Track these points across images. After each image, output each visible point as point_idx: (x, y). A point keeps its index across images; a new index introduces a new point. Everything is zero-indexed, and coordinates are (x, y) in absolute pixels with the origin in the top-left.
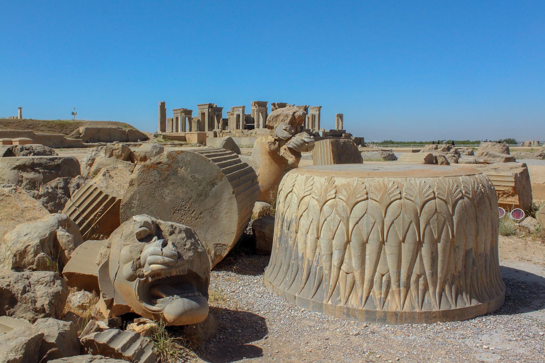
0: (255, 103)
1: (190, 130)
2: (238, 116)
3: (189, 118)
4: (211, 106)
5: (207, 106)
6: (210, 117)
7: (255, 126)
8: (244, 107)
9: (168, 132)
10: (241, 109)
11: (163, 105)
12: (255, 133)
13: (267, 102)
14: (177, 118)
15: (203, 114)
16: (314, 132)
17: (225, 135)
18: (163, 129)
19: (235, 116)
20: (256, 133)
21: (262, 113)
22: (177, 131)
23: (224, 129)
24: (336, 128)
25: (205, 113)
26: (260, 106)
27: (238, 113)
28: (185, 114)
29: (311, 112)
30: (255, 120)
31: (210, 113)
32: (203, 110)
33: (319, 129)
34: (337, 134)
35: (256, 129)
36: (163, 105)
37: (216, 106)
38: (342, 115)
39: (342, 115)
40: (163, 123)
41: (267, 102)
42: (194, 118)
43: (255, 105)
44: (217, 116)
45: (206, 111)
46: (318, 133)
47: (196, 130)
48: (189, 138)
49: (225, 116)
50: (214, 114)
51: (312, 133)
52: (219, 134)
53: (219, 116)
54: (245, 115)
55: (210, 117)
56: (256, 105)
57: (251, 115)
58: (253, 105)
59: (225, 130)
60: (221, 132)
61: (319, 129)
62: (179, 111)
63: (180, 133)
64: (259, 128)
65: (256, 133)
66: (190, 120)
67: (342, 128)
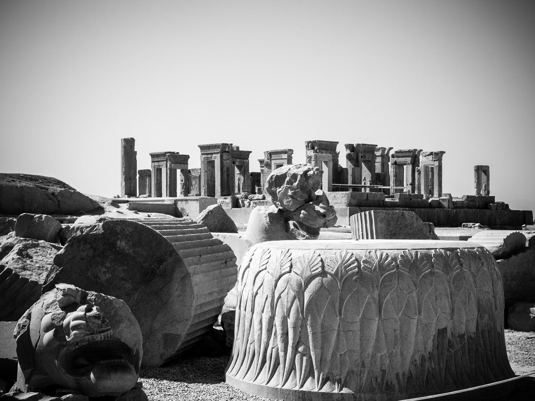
3: (182, 171)
5: (219, 150)
6: (225, 169)
9: (142, 199)
14: (159, 171)
15: (210, 164)
16: (430, 201)
17: (254, 203)
21: (326, 163)
22: (159, 194)
23: (254, 192)
24: (473, 192)
26: (323, 149)
31: (225, 162)
33: (440, 195)
37: (238, 148)
38: (488, 167)
39: (488, 167)
42: (193, 170)
44: (239, 167)
48: (183, 209)
49: (254, 167)
50: (234, 163)
52: (243, 202)
53: (244, 168)
55: (225, 169)
59: (255, 193)
60: (246, 198)
61: (440, 195)
63: (166, 200)
66: (186, 173)
67: (489, 192)
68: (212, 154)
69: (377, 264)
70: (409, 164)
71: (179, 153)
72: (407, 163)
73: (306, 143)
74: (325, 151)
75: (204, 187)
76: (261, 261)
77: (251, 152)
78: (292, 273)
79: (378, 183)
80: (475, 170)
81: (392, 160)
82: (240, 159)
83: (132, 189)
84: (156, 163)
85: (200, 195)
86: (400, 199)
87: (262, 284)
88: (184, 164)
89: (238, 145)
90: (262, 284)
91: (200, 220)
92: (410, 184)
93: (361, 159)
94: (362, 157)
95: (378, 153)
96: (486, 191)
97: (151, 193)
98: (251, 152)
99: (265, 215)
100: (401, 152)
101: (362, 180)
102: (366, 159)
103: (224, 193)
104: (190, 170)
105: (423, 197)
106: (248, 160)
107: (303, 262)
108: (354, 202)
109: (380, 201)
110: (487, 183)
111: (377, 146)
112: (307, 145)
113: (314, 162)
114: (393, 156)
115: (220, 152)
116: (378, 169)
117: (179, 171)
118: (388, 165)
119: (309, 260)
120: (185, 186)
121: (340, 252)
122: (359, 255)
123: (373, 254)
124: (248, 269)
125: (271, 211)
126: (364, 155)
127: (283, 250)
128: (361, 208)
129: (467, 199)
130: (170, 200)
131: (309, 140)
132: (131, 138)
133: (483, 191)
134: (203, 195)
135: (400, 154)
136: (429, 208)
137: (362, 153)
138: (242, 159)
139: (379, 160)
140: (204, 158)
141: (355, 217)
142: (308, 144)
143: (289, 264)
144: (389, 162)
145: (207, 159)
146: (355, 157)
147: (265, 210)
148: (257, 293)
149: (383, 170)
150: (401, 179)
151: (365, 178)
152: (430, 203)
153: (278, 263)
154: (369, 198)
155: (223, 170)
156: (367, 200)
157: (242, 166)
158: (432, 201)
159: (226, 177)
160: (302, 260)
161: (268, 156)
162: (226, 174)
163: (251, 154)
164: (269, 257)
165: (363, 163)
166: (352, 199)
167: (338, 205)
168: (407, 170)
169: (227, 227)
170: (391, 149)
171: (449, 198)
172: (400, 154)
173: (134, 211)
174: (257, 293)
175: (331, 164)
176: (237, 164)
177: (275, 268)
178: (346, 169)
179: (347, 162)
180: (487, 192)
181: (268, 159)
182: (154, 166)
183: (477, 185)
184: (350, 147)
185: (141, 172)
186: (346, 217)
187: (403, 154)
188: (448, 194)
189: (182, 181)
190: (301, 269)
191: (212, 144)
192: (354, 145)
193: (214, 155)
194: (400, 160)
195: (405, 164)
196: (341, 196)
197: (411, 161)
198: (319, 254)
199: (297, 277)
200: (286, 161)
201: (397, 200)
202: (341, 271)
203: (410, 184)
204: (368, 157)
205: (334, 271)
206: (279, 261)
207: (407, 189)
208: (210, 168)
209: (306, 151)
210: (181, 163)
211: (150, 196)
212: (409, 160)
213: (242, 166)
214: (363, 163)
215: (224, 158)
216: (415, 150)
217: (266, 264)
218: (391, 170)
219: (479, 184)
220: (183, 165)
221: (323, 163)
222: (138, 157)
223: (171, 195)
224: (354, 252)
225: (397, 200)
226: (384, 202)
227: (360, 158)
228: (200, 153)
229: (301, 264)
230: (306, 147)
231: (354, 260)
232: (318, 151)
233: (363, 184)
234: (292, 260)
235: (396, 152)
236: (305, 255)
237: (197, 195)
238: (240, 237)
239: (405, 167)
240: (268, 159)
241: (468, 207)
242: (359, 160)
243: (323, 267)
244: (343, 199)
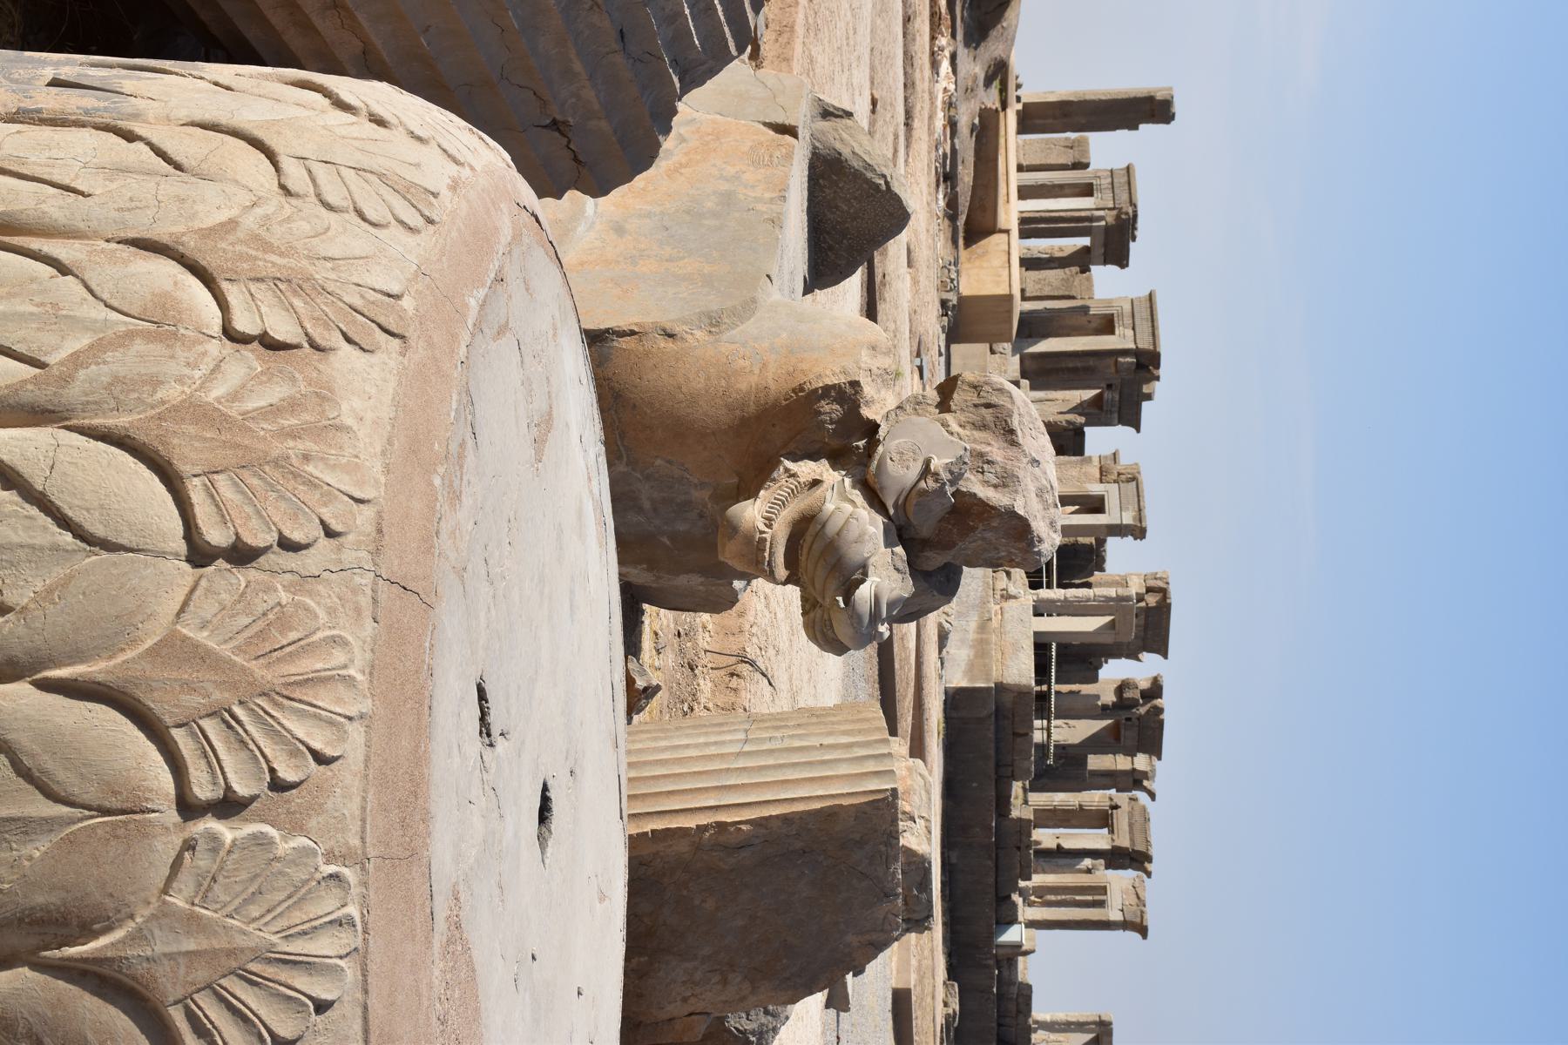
0: (1164, 592)
1: (1029, 263)
2: (1094, 505)
4: (1147, 363)
5: (1145, 344)
6: (1091, 362)
7: (1044, 593)
8: (1138, 532)
9: (1013, 146)
10: (1128, 519)
11: (1155, 109)
12: (1012, 590)
13: (1165, 656)
14: (1087, 190)
15: (1107, 325)
16: (1016, 897)
18: (1035, 118)
19: (1095, 488)
20: (1007, 597)
21: (1112, 624)
22: (1025, 193)
25: (1112, 332)
26: (1147, 617)
27: (1112, 503)
28: (1107, 228)
29: (1119, 881)
30: (1072, 593)
31: (1111, 361)
32: (1128, 321)
33: (1032, 924)
35: (1028, 597)
36: (1155, 109)
37: (1149, 397)
40: (1065, 115)
41: (1165, 656)
42: (1089, 280)
43: (1149, 590)
44: (1097, 401)
45: (1121, 339)
46: (1012, 920)
47: (1028, 295)
49: (1099, 440)
50: (1109, 386)
51: (1016, 888)
53: (1097, 413)
54: (1101, 543)
55: (1091, 362)
56: (1152, 600)
57: (1102, 570)
58: (1152, 583)
61: (1032, 924)
62: (1125, 197)
63: (1011, 210)
64: (1037, 613)
65: (1007, 597)
66: (1082, 261)
68: (1134, 329)
69: (241, 941)
70: (1113, 840)
71: (1134, 240)
72: (1115, 837)
73: (1164, 572)
74: (1142, 622)
76: (346, 172)
77: (1138, 430)
78: (218, 348)
79: (1061, 762)
81: (1122, 798)
82: (1120, 401)
83: (1038, 122)
84: (1109, 180)
85: (1024, 298)
86: (1020, 820)
87: (178, 167)
88: (1105, 254)
89: (1156, 396)
90: (178, 167)
91: (854, 144)
92: (1059, 846)
93: (1124, 718)
94: (1128, 719)
95: (1141, 762)
97: (1027, 171)
98: (1138, 430)
99: (851, 366)
100: (1147, 820)
101: (1066, 721)
102: (1123, 732)
103: (1027, 363)
104: (1090, 271)
105: (1023, 880)
106: (1116, 421)
107: (290, 421)
108: (1008, 699)
109: (1010, 769)
112: (1158, 576)
113: (1115, 596)
114: (1133, 799)
115: (1137, 347)
116: (1096, 762)
117: (1085, 241)
118: (1109, 789)
119: (294, 461)
120: (1045, 259)
121: (352, 672)
122: (316, 808)
123: (326, 905)
124: (326, 102)
125: (868, 390)
127: (407, 303)
128: (993, 716)
130: (1008, 221)
131: (1170, 581)
132: (1174, 114)
134: (1020, 306)
135: (1138, 818)
136: (997, 894)
137: (1138, 719)
138: (1120, 408)
139: (1122, 763)
141: (874, 718)
142: (1160, 579)
143: (283, 330)
144: (1117, 791)
145: (1118, 316)
147: (875, 370)
148: (130, 137)
149: (1094, 775)
150: (1073, 822)
151: (1074, 727)
152: (1010, 897)
153: (305, 263)
154: (1019, 740)
156: (1014, 734)
157: (1100, 408)
158: (1014, 905)
159: (1071, 365)
160: (306, 417)
161: (1129, 474)
162: (1079, 365)
163: (1131, 430)
164: (364, 219)
165: (1110, 721)
166: (1015, 694)
167: (1000, 658)
168: (1097, 839)
169: (831, 248)
170: (1152, 796)
171: (1024, 948)
172: (1138, 818)
173: (977, 121)
174: (130, 137)
175: (1108, 639)
176: (1106, 395)
177: (267, 247)
178: (1094, 679)
179: (1114, 681)
181: (1119, 474)
182: (1099, 177)
184: (1155, 690)
185: (1083, 144)
186: (966, 680)
187: (1137, 827)
188: (1035, 946)
189: (1061, 250)
190: (233, 411)
192: (1159, 700)
193: (1130, 333)
194: (1121, 820)
195: (1112, 832)
196: (1023, 666)
197: (1120, 848)
198: (336, 526)
199: (180, 380)
200: (1118, 522)
201: (1015, 813)
202: (189, 687)
203: (1059, 846)
204: (1129, 736)
205: (202, 637)
206: (322, 273)
207: (1045, 837)
208: (1094, 325)
209: (1138, 575)
210: (1106, 245)
211: (1020, 168)
212: (1124, 841)
213: (1100, 408)
214: (1110, 721)
215: (1120, 359)
216: (1149, 859)
217: (318, 195)
218: (1095, 798)
221: (1112, 617)
222: (1122, 135)
223: (1024, 221)
224: (348, 774)
225: (1015, 813)
226: (1008, 777)
227: (1124, 715)
228: (1134, 296)
229: (273, 411)
230: (1152, 574)
231: (272, 771)
232: (1142, 604)
233: (1054, 723)
234: (317, 355)
235: (1144, 809)
236: (345, 437)
237: (1023, 291)
238: (768, 276)
239: (1105, 831)
240: (1119, 474)
242: (1121, 713)
243: (241, 555)
244: (1015, 671)
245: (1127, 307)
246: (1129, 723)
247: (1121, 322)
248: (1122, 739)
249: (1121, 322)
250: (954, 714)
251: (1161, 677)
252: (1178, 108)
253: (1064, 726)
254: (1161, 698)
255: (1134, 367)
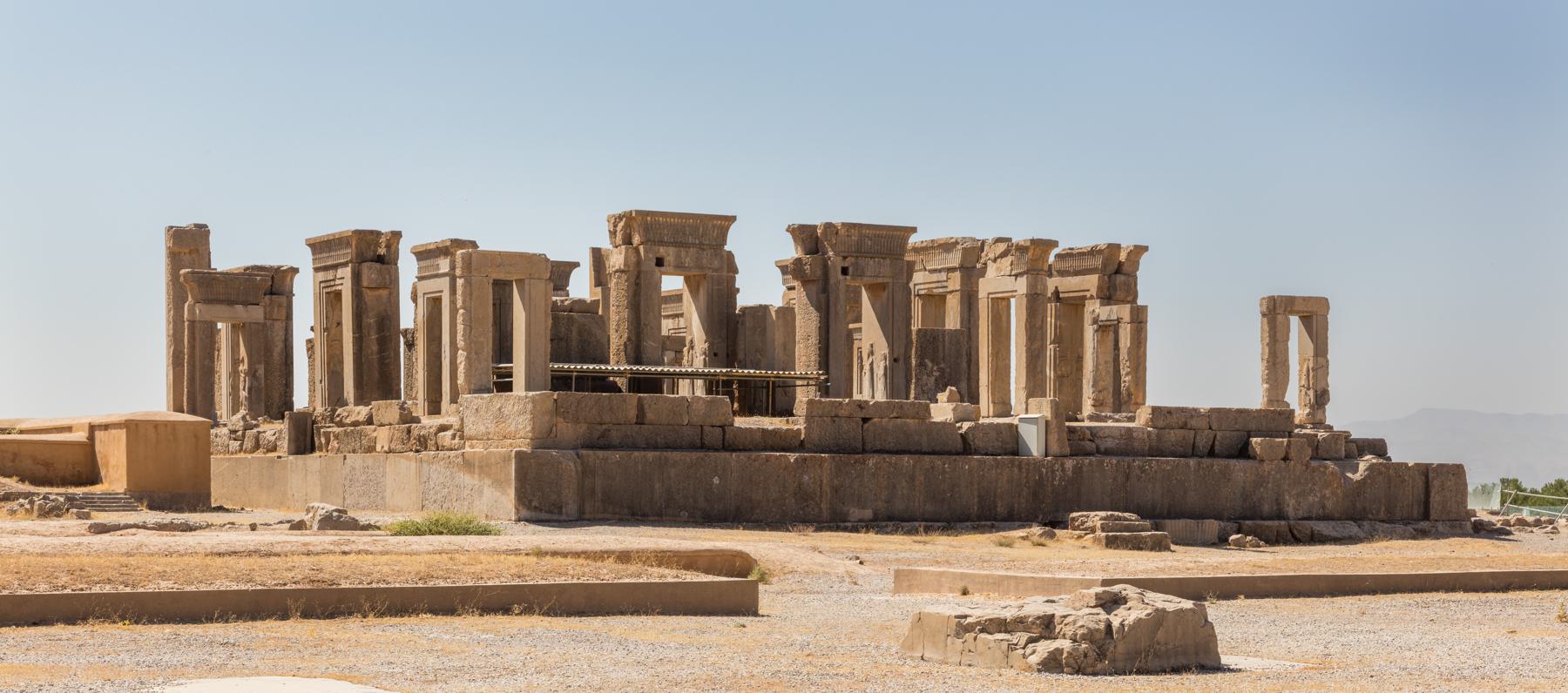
6: (371, 320)
31: (369, 296)
32: (330, 275)
34: (1203, 442)
55: (371, 320)
75: (321, 381)
80: (1264, 315)
93: (841, 277)
94: (845, 271)
96: (1311, 393)
110: (1316, 362)
111: (914, 230)
115: (351, 261)
120: (251, 381)
126: (856, 265)
129: (1151, 419)
133: (1304, 390)
140: (320, 282)
146: (819, 273)
151: (872, 346)
155: (364, 324)
159: (375, 348)
162: (374, 337)
180: (1316, 396)
183: (1268, 368)
186: (509, 491)
191: (334, 235)
210: (231, 303)
215: (365, 283)
219: (1274, 364)
220: (239, 308)
241: (1157, 451)
242: (832, 281)
245: (321, 276)
246: (851, 270)
247: (332, 283)
248: (880, 280)
249: (332, 283)
250: (571, 508)
251: (789, 226)
252: (185, 221)
253: (870, 359)
254: (815, 227)
255: (378, 265)
